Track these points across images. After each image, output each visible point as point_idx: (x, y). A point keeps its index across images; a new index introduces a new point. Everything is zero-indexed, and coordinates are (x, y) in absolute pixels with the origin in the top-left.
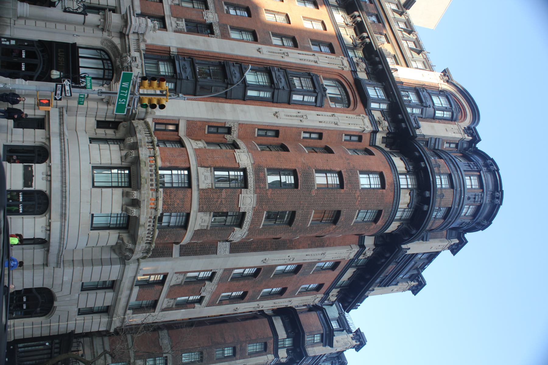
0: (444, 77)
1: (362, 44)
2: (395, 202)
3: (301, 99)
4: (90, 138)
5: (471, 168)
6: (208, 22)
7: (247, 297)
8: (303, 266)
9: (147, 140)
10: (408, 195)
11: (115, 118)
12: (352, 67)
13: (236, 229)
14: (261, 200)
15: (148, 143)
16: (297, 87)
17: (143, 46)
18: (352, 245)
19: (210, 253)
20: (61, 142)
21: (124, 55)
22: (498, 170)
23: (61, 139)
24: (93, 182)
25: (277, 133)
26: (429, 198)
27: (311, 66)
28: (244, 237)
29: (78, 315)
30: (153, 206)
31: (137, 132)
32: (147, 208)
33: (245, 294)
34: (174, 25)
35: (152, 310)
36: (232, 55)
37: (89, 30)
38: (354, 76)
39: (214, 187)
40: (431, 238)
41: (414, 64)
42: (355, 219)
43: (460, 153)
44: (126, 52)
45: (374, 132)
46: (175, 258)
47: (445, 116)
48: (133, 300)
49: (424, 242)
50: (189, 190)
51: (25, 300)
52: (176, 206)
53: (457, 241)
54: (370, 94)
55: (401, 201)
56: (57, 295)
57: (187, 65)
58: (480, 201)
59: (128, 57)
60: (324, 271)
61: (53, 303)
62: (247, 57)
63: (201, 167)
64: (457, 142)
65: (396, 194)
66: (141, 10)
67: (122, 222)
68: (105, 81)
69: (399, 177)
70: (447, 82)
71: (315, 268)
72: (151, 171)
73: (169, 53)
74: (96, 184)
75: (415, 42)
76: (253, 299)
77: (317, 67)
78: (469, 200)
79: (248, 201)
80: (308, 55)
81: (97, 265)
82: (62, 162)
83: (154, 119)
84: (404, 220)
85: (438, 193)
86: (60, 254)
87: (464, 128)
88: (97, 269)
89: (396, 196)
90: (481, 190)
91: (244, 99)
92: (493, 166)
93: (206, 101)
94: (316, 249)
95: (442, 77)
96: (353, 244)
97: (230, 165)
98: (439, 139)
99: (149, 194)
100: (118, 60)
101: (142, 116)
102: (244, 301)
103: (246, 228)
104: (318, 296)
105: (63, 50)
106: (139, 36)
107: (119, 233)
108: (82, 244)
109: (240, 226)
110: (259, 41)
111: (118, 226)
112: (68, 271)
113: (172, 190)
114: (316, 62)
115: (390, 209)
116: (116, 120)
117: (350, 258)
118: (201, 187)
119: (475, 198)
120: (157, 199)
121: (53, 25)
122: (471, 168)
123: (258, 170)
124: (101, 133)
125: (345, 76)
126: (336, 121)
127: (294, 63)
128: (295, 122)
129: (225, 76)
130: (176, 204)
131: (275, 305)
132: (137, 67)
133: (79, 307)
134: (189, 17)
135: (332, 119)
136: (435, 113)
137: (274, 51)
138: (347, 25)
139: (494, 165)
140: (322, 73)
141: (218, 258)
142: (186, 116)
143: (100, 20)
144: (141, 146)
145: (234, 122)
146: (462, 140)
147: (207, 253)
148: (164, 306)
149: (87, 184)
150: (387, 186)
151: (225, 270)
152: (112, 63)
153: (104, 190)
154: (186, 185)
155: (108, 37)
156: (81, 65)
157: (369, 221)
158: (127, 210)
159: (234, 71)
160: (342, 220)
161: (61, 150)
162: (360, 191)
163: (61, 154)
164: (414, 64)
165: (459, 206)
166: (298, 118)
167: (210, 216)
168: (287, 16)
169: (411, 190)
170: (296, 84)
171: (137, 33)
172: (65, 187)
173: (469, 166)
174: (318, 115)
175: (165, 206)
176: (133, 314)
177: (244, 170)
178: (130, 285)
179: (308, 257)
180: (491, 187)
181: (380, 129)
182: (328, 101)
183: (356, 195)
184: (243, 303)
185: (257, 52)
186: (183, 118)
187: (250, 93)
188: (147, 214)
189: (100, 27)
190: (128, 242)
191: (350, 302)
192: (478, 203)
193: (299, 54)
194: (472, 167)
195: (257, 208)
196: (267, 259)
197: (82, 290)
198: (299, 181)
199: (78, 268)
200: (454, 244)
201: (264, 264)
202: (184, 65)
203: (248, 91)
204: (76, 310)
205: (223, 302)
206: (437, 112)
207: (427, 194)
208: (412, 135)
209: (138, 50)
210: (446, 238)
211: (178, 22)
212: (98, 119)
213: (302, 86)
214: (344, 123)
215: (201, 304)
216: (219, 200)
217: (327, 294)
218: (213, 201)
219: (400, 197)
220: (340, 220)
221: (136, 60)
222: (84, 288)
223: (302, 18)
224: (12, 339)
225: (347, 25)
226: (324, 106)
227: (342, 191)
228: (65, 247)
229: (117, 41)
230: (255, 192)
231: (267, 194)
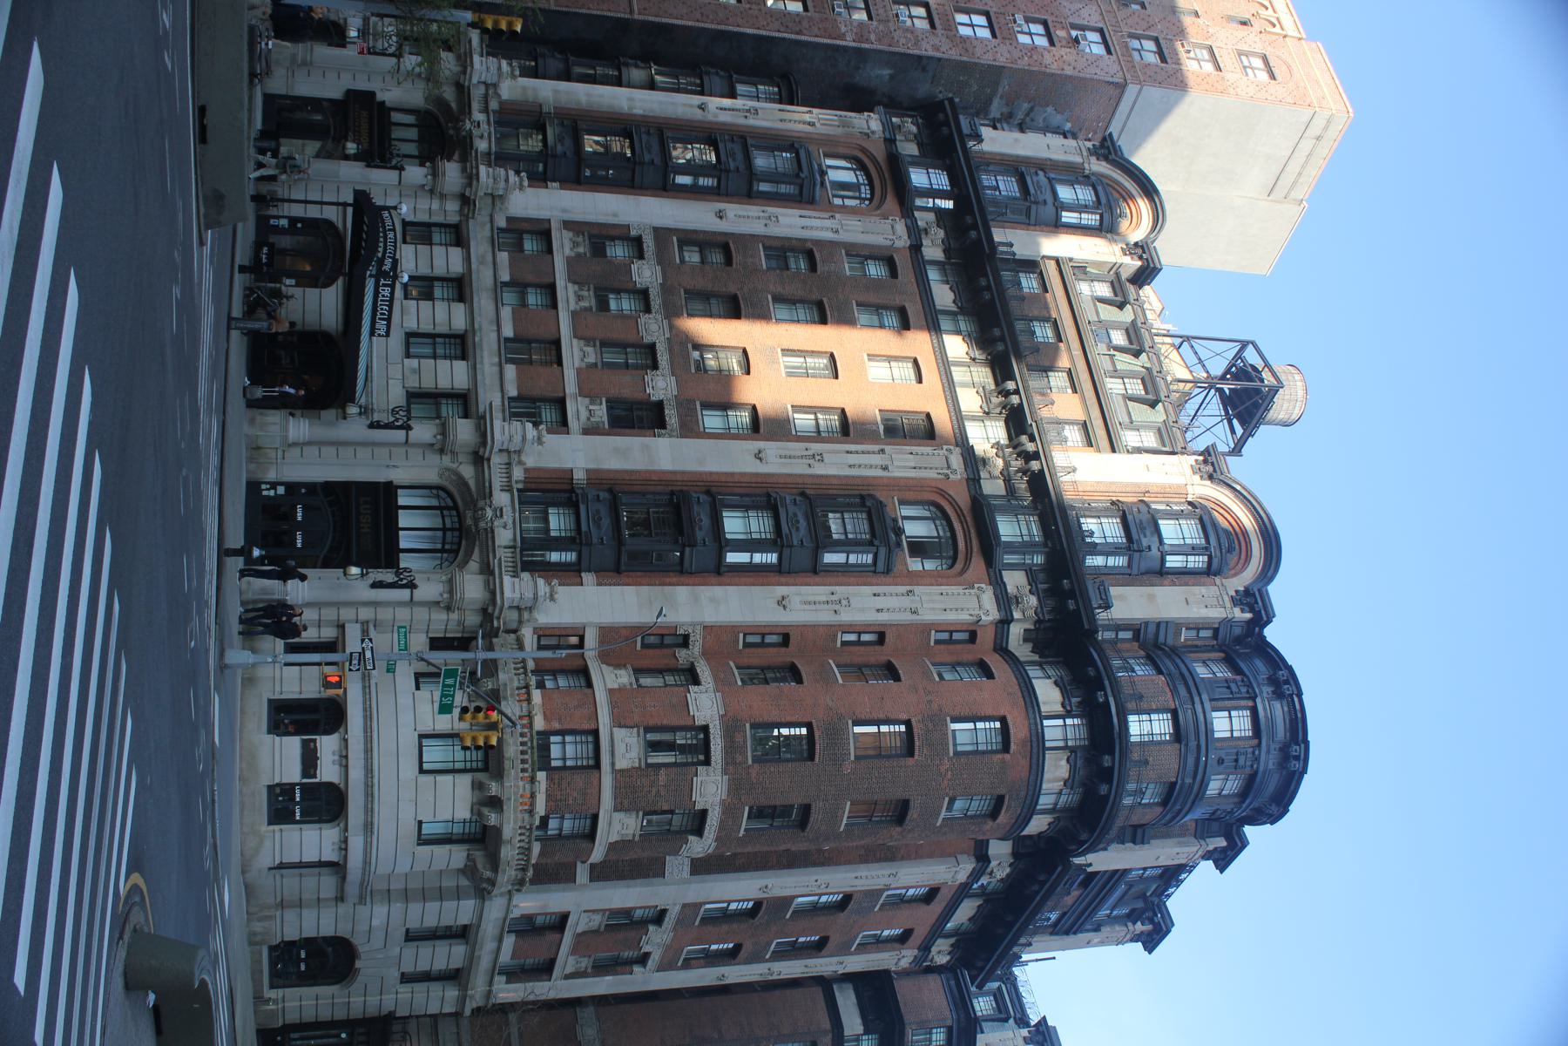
0: (1202, 466)
1: (1004, 408)
2: (1032, 778)
3: (844, 561)
4: (415, 674)
5: (1232, 693)
6: (653, 398)
7: (743, 954)
8: (854, 897)
9: (516, 684)
10: (1064, 762)
11: (463, 632)
12: (970, 470)
13: (691, 838)
14: (735, 787)
15: (518, 688)
16: (835, 536)
17: (518, 474)
18: (959, 857)
19: (651, 874)
20: (364, 693)
21: (481, 503)
22: (1300, 695)
23: (364, 687)
24: (421, 762)
25: (786, 640)
26: (1111, 769)
27: (874, 478)
28: (710, 851)
29: (401, 982)
30: (526, 808)
31: (500, 667)
32: (515, 812)
33: (738, 948)
34: (584, 414)
35: (545, 977)
36: (701, 474)
37: (416, 454)
38: (973, 492)
39: (643, 765)
40: (1155, 837)
41: (1130, 438)
42: (943, 814)
43: (1220, 651)
45: (1005, 622)
46: (580, 885)
47: (1190, 565)
48: (505, 957)
49: (1137, 847)
50: (595, 772)
51: (303, 955)
52: (571, 802)
53: (1221, 842)
54: (1002, 532)
55: (1046, 776)
56: (361, 949)
57: (604, 512)
58: (1252, 766)
59: (488, 509)
60: (907, 905)
61: (353, 963)
62: (733, 474)
63: (620, 726)
64: (1217, 626)
65: (1034, 761)
66: (519, 388)
67: (473, 830)
68: (445, 555)
69: (1042, 724)
70: (1211, 477)
71: (882, 899)
72: (523, 744)
73: (570, 487)
74: (426, 766)
75: (1146, 379)
76: (756, 958)
77: (889, 478)
78: (1223, 766)
79: (711, 789)
80: (868, 453)
81: (433, 900)
82: (365, 732)
83: (535, 629)
84: (1065, 810)
85: (1135, 756)
86: (363, 884)
87: (1237, 592)
88: (433, 906)
89: (1034, 767)
90: (1256, 741)
91: (719, 571)
92: (1289, 683)
93: (641, 584)
94: (876, 865)
95: (1198, 466)
96: (961, 853)
97: (675, 722)
98: (1167, 622)
99: (518, 787)
100: (469, 514)
101: (514, 626)
102: (736, 961)
103: (711, 836)
104: (904, 952)
106: (510, 457)
107: (468, 850)
108: (403, 867)
109: (699, 832)
110: (762, 431)
111: (466, 837)
112: (380, 911)
113: (564, 774)
114: (885, 468)
115: (1023, 794)
116: (465, 635)
117: (958, 883)
118: (618, 767)
119: (1236, 761)
120: (533, 796)
121: (351, 449)
122: (1232, 693)
123: (731, 727)
124: (439, 657)
125: (952, 494)
126: (913, 606)
127: (834, 476)
128: (824, 616)
129: (680, 530)
130: (571, 798)
131: (806, 970)
132: (505, 527)
133: (402, 970)
134: (614, 392)
135: (906, 602)
136: (1163, 561)
137: (792, 453)
138: (974, 359)
139: (1292, 682)
140: (899, 490)
141: (666, 884)
142: (597, 620)
143: (435, 437)
144: (505, 698)
145: (694, 625)
146: (1227, 622)
147: (646, 876)
148: (569, 969)
149: (409, 767)
150: (1013, 747)
151: (684, 906)
152: (459, 516)
153: (440, 778)
154: (591, 762)
155: (451, 465)
156: (400, 525)
157: (980, 815)
158: (480, 814)
159: (699, 514)
160: (915, 816)
161: (365, 710)
162: (950, 759)
163: (365, 717)
164: (1130, 438)
165: (1194, 778)
166: (830, 606)
167: (637, 817)
168: (832, 356)
169: (1071, 752)
170: (833, 528)
171: (508, 451)
172: (372, 778)
173: (1229, 687)
174: (875, 595)
175: (551, 803)
176: (508, 982)
177: (705, 729)
178: (497, 932)
179: (857, 882)
180: (1281, 732)
181: (1017, 615)
182: (905, 557)
183: (943, 769)
184: (734, 965)
185: (754, 459)
186: (591, 624)
187: (732, 557)
188: (515, 822)
189: (436, 447)
190: (484, 868)
191: (982, 969)
192: (1248, 771)
193: (848, 452)
194: (1234, 689)
195: (729, 800)
196: (770, 886)
197: (406, 941)
198: (817, 746)
199: (398, 905)
200: (1216, 849)
201: (766, 896)
202: (598, 512)
203: (728, 554)
204: (397, 975)
205: (693, 962)
206: (1168, 558)
207: (1107, 761)
208: (1086, 627)
209: (508, 488)
210: (1195, 837)
211: (591, 407)
212: (431, 635)
213: (846, 533)
214: (934, 609)
215: (645, 967)
216: (654, 790)
217: (925, 948)
218: (641, 791)
219: (1043, 769)
220: (908, 817)
221: (501, 516)
222: (411, 937)
223: (866, 357)
224: (280, 1024)
225: (974, 359)
226: (895, 570)
227: (910, 761)
228: (373, 869)
229: (467, 471)
230: (725, 772)
231: (749, 774)
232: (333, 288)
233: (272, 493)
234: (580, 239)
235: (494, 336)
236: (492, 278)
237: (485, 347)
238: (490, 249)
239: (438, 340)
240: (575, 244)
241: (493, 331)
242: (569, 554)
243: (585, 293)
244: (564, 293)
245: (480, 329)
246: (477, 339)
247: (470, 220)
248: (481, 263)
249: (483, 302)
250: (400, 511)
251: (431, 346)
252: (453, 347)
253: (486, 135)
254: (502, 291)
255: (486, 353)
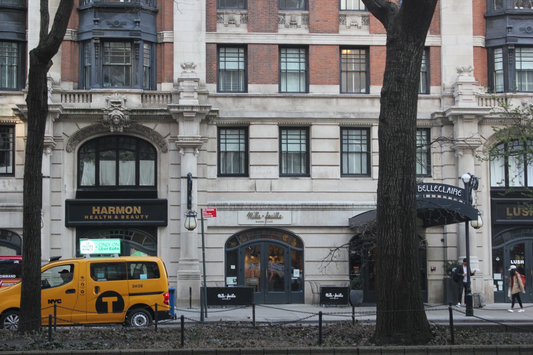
21: (523, 122)
44: (520, 120)
105: (508, 209)
202: (521, 29)
232: (302, 237)
233: (500, 283)
234: (226, 18)
235: (342, 102)
236: (280, 100)
237: (356, 110)
238: (247, 100)
239: (345, 149)
240: (232, 22)
241: (337, 103)
242: (496, 56)
243: (288, 19)
244: (291, 37)
245: (341, 113)
246: (352, 117)
247: (221, 115)
248: (265, 109)
249: (308, 109)
250: (529, 185)
251: (350, 156)
252: (350, 137)
253: (124, 96)
254: (287, 92)
255: (362, 110)
